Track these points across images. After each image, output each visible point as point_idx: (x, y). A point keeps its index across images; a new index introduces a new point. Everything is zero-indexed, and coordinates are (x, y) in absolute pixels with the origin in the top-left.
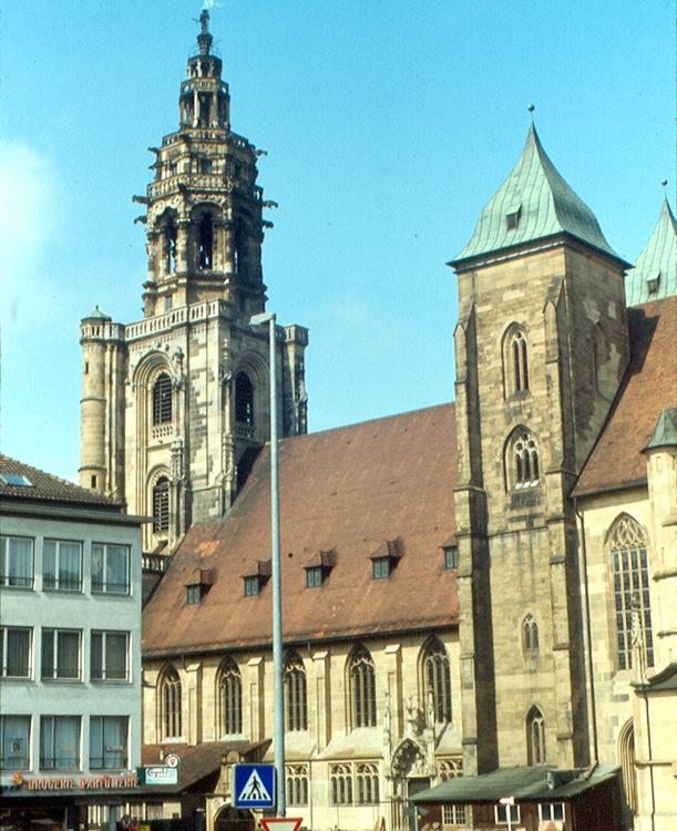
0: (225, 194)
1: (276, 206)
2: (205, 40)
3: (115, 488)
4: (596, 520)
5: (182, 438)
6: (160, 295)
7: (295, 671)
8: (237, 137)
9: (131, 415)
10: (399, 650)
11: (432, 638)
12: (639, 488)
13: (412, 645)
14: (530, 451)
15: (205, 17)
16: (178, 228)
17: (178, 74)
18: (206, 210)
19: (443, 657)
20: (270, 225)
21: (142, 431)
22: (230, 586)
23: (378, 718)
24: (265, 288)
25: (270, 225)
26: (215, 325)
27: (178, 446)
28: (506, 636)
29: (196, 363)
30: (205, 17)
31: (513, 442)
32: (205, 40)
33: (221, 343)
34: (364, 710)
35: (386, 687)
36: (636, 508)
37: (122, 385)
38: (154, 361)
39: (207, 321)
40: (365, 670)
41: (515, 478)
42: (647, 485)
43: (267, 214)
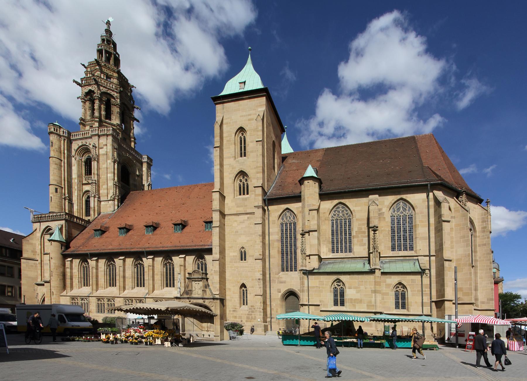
0: (117, 93)
3: (67, 195)
4: (276, 210)
5: (96, 179)
6: (88, 125)
7: (139, 264)
9: (75, 169)
10: (185, 258)
11: (201, 253)
12: (297, 198)
13: (191, 255)
14: (245, 183)
19: (204, 262)
21: (80, 176)
22: (114, 231)
23: (175, 284)
26: (110, 138)
27: (94, 182)
28: (232, 254)
29: (102, 151)
31: (238, 178)
33: (113, 146)
34: (170, 282)
35: (179, 271)
36: (294, 206)
37: (69, 157)
38: (84, 150)
39: (107, 135)
40: (170, 265)
41: (238, 193)
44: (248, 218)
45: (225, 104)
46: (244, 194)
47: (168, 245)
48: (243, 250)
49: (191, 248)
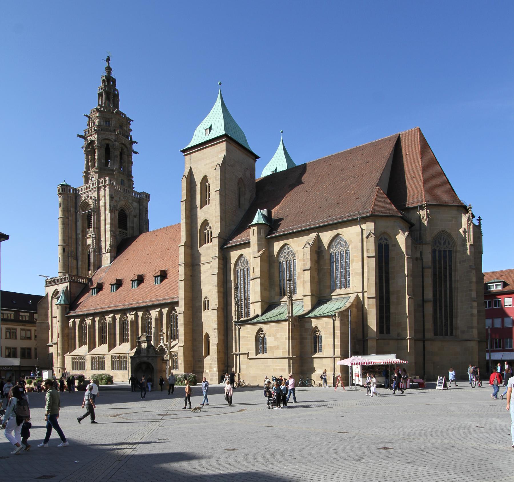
1: (137, 143)
2: (109, 69)
8: (121, 113)
12: (247, 244)
14: (210, 230)
15: (108, 59)
16: (95, 149)
17: (98, 86)
18: (107, 142)
20: (137, 153)
24: (133, 177)
25: (137, 153)
30: (108, 59)
32: (109, 69)
36: (244, 251)
42: (249, 243)
43: (135, 147)
44: (211, 266)
45: (193, 154)
46: (208, 242)
47: (147, 301)
48: (206, 300)
49: (164, 302)
